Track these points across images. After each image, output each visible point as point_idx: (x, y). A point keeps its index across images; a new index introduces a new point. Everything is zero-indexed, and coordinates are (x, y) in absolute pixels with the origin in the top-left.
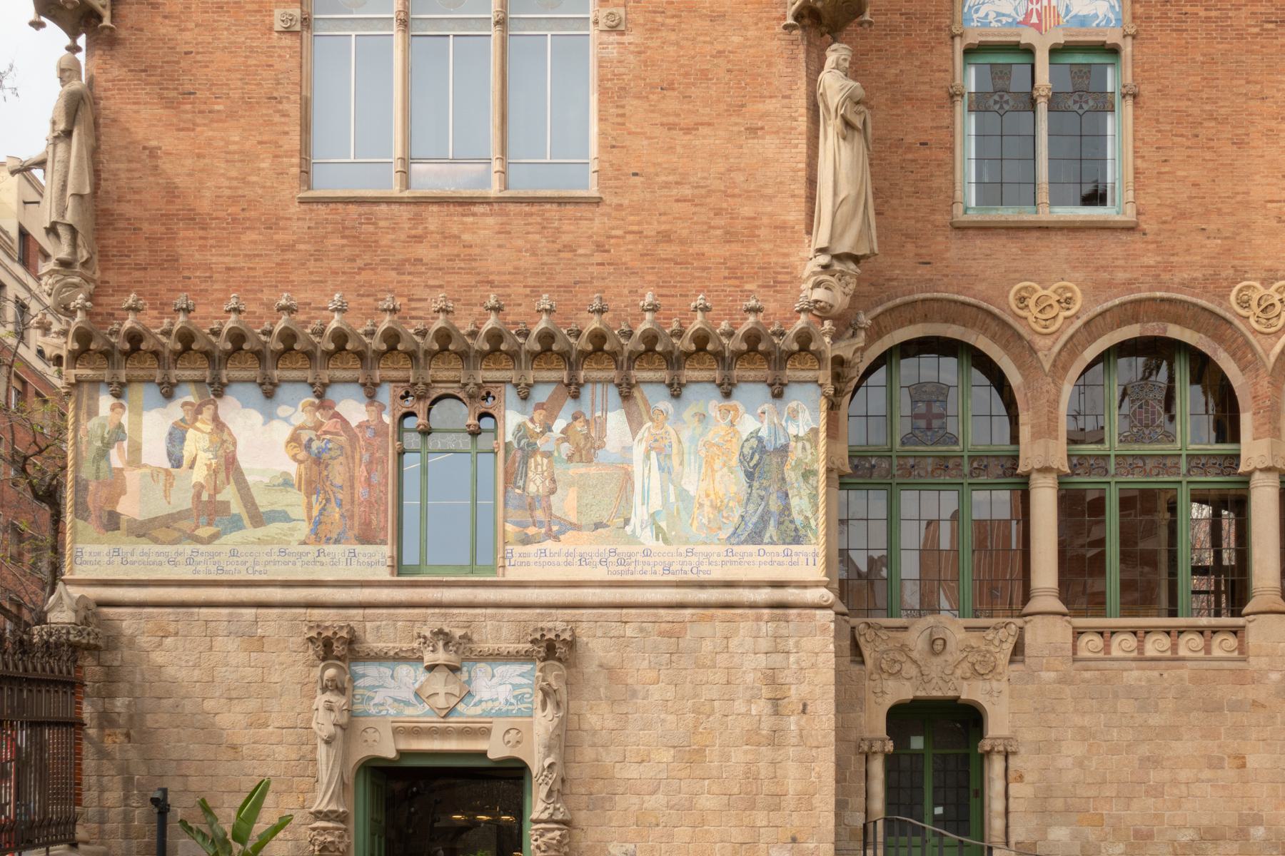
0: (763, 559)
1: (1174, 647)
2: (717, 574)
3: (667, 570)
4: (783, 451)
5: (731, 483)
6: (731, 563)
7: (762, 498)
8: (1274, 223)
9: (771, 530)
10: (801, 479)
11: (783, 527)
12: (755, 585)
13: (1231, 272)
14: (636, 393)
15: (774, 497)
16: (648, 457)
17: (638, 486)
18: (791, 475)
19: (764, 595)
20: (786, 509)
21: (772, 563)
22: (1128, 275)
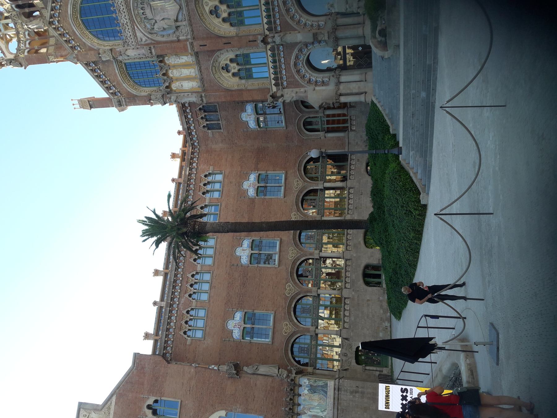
0: (330, 391)
1: (348, 310)
2: (332, 400)
3: (331, 410)
4: (311, 385)
5: (316, 396)
6: (330, 397)
7: (319, 390)
8: (276, 288)
9: (325, 389)
10: (316, 383)
11: (324, 387)
12: (334, 393)
13: (284, 296)
14: (299, 412)
15: (319, 388)
16: (310, 411)
17: (316, 414)
18: (315, 385)
19: (336, 392)
20: (322, 386)
21: (331, 390)
22: (283, 313)
